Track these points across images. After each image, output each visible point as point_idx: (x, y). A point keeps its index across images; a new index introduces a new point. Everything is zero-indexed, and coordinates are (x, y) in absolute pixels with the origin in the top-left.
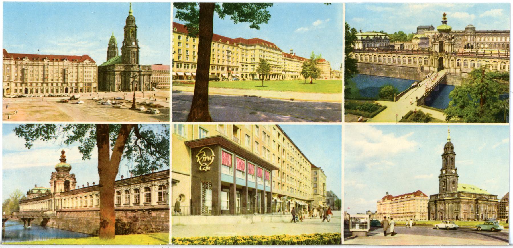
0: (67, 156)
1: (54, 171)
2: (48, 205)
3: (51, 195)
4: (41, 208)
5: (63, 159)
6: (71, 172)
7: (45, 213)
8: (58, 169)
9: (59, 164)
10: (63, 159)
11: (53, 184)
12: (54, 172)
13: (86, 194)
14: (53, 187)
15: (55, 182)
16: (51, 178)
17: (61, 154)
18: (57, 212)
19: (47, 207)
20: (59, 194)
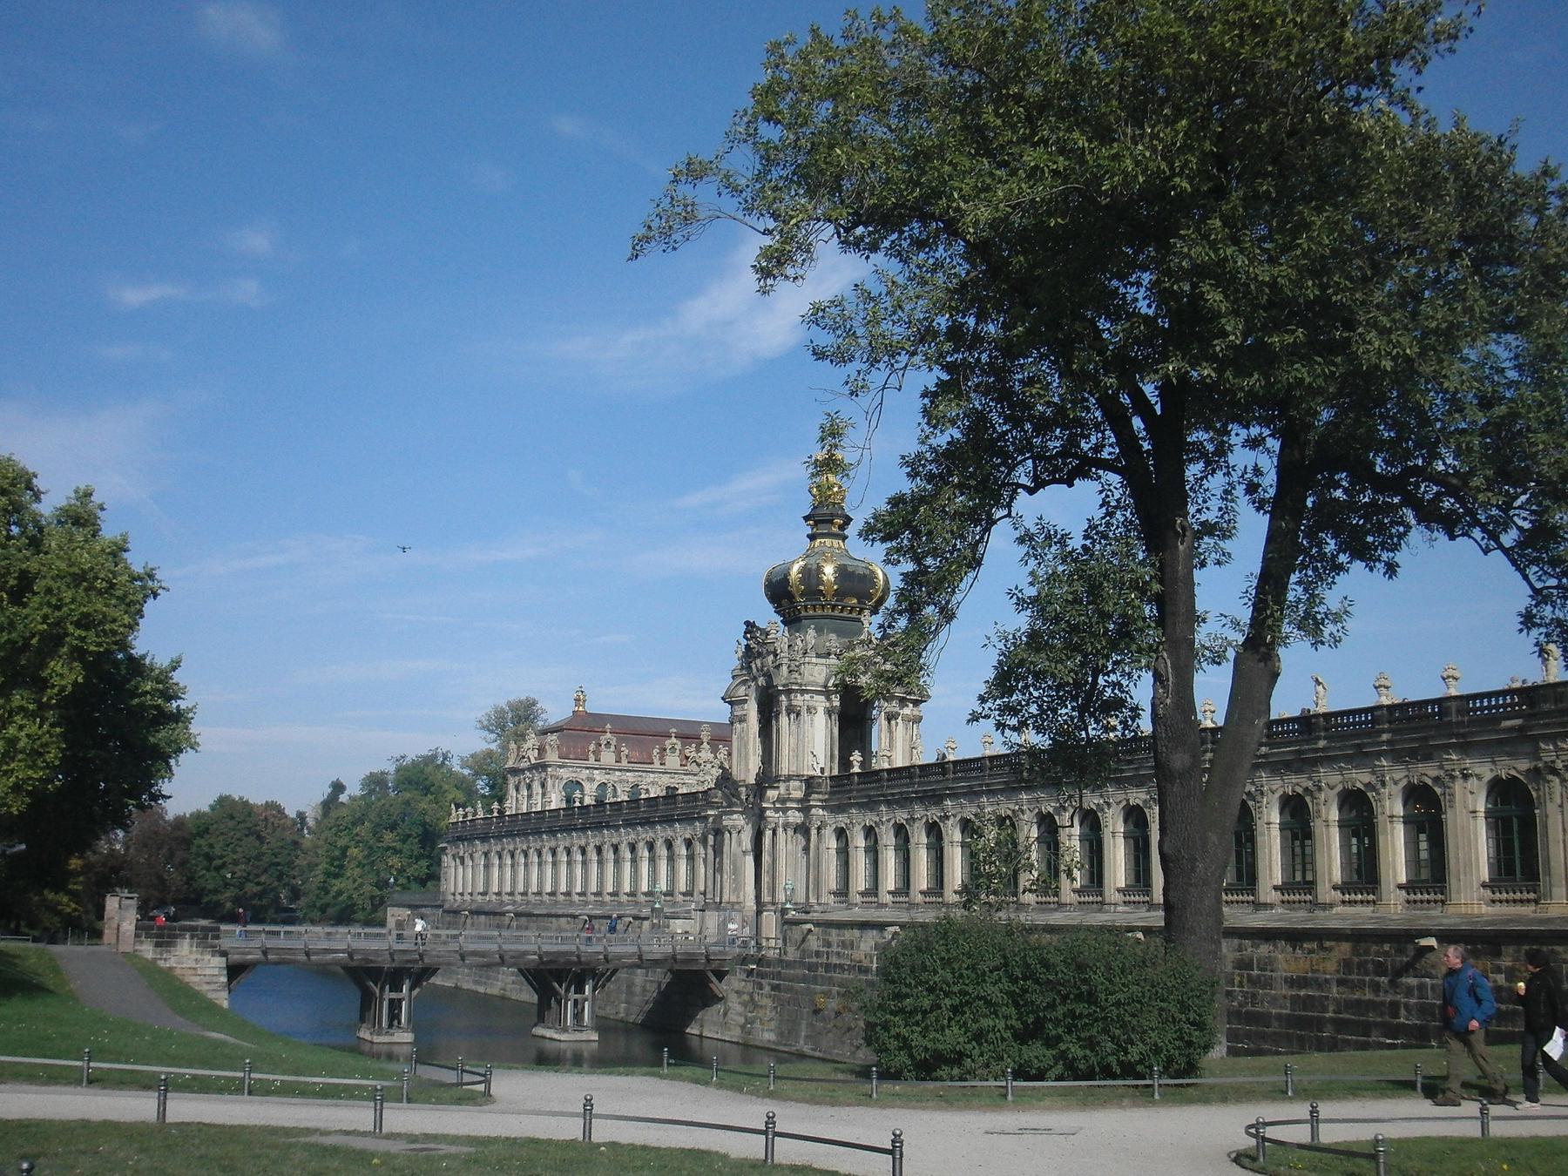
11: (752, 710)
12: (761, 624)
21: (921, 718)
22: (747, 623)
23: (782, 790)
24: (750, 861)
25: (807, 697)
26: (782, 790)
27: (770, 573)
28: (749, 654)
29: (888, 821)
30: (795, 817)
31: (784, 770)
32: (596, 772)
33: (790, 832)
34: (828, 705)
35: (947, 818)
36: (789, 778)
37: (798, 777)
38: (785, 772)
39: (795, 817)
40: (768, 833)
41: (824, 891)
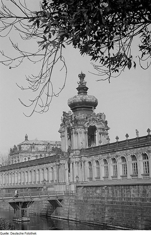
0: (89, 82)
1: (68, 110)
2: (55, 173)
3: (62, 153)
4: (42, 179)
5: (83, 89)
6: (97, 111)
7: (50, 189)
8: (74, 106)
9: (75, 97)
10: (83, 89)
11: (66, 133)
13: (134, 152)
14: (66, 137)
15: (69, 130)
16: (61, 122)
17: (79, 80)
18: (77, 187)
19: (56, 178)
20: (78, 152)
21: (108, 133)
22: (63, 112)
23: (74, 153)
24: (67, 171)
25: (79, 129)
26: (74, 153)
27: (69, 100)
28: (64, 121)
29: (102, 159)
30: (77, 160)
31: (75, 147)
32: (31, 154)
33: (77, 164)
34: (85, 131)
35: (118, 157)
36: (76, 150)
37: (78, 150)
38: (75, 148)
39: (77, 160)
40: (71, 165)
41: (86, 178)
